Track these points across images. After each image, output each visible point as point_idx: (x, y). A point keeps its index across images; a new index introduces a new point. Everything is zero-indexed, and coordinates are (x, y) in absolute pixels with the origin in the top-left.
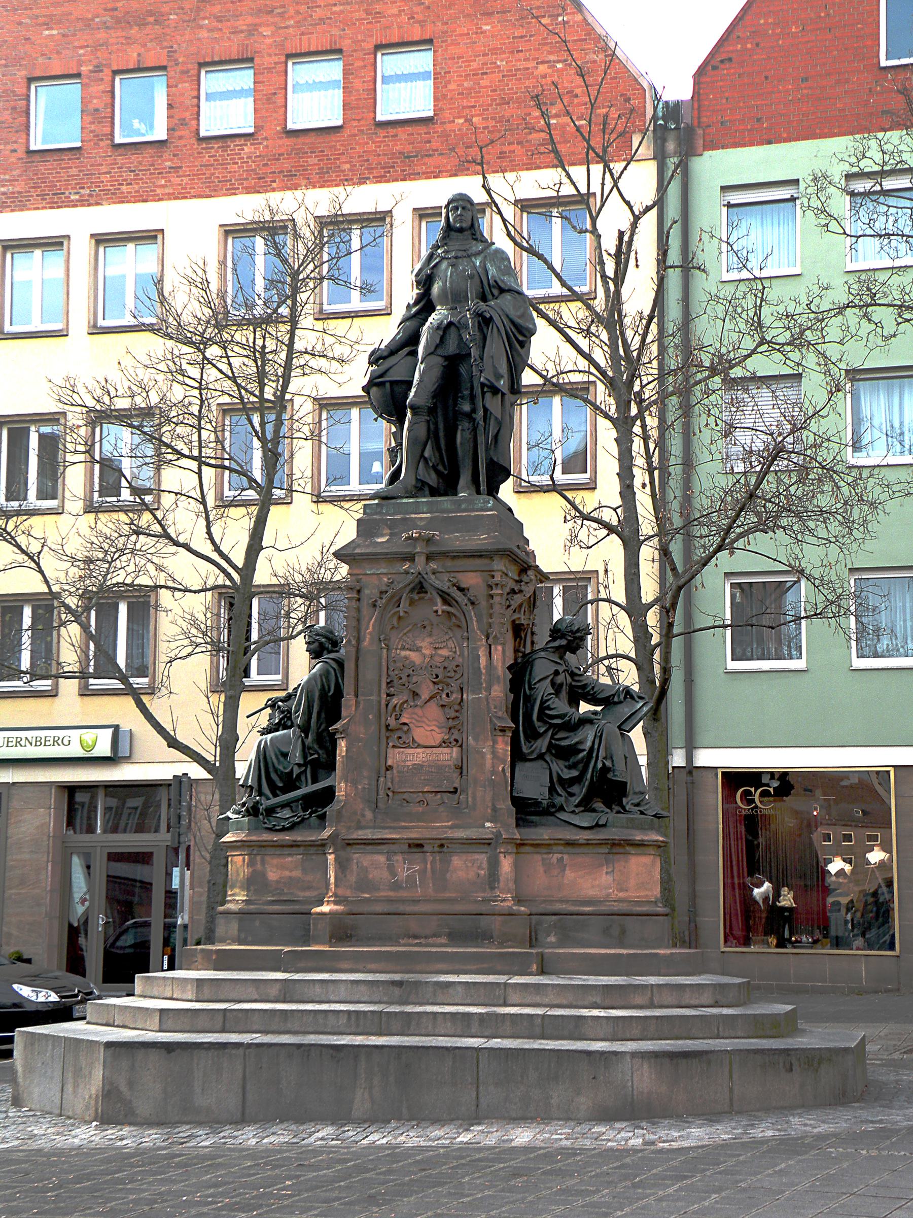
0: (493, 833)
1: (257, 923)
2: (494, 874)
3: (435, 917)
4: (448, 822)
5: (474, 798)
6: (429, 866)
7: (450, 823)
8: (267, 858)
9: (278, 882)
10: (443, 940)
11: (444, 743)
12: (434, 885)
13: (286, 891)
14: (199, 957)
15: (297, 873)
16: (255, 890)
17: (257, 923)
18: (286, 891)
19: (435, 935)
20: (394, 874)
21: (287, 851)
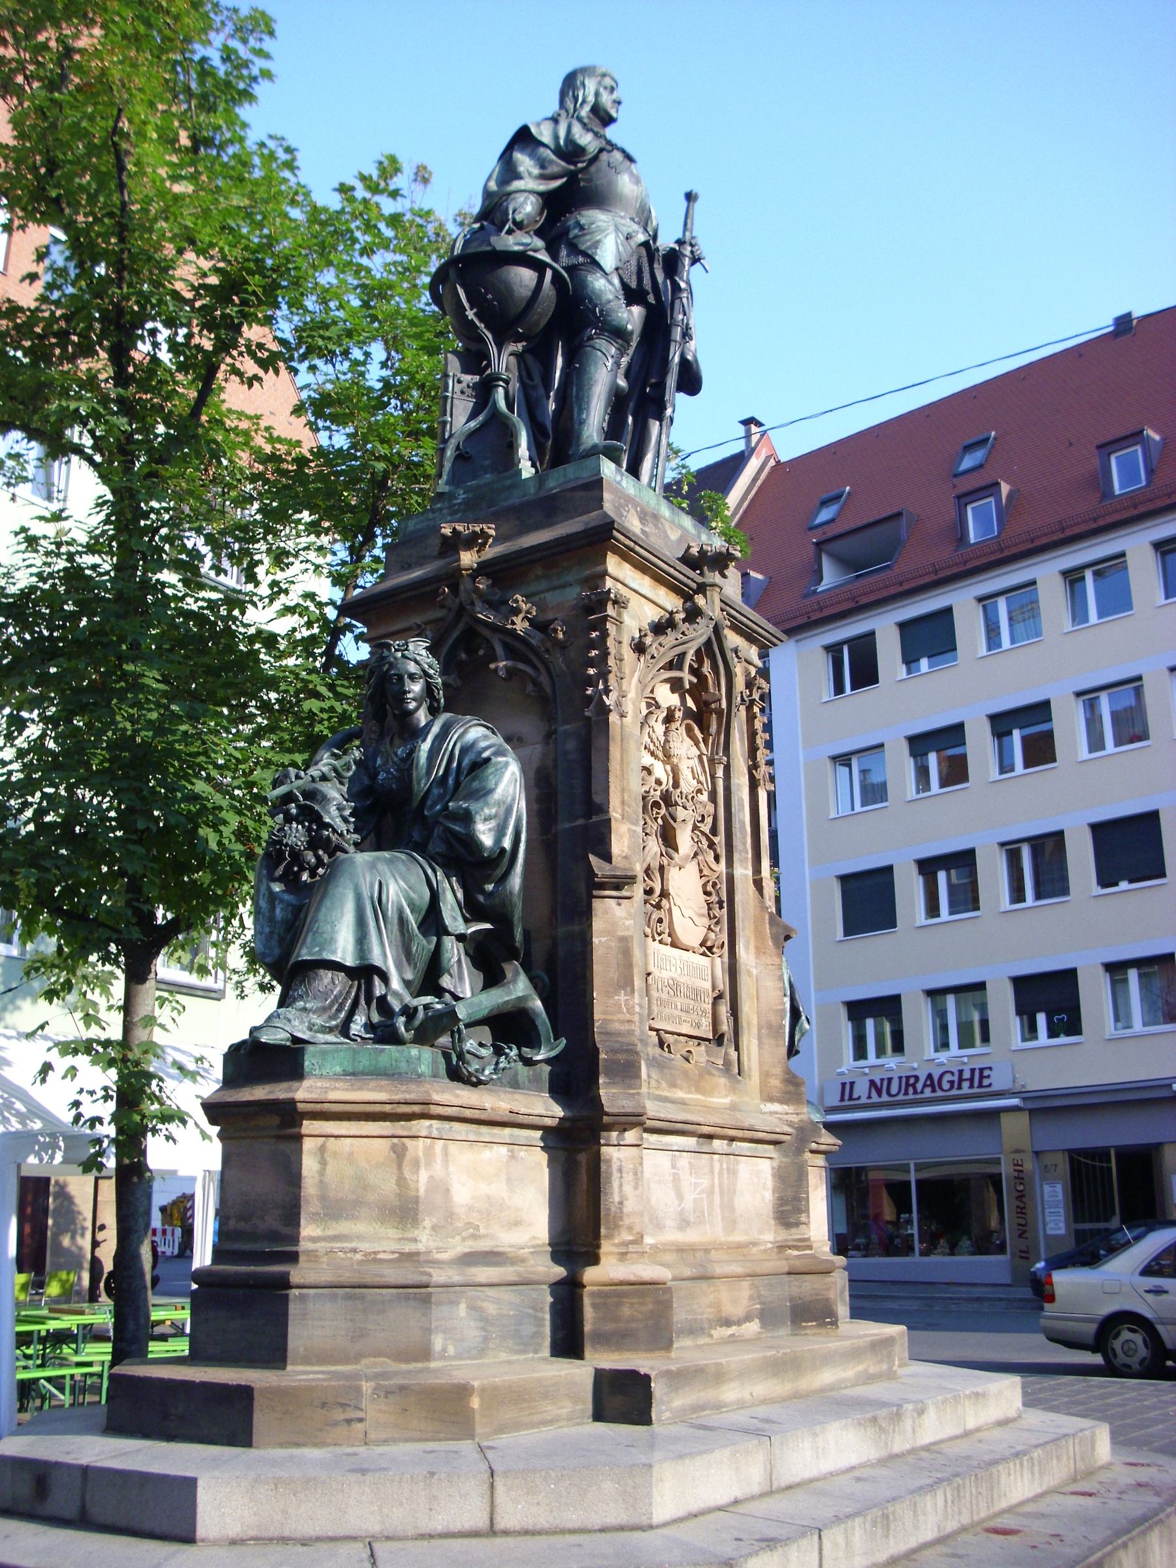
0: (790, 1124)
1: (462, 1309)
2: (797, 1199)
3: (746, 1284)
4: (726, 1096)
5: (749, 1060)
6: (716, 1181)
7: (727, 1101)
8: (453, 1147)
9: (471, 1208)
10: (753, 1327)
11: (708, 949)
12: (723, 1219)
13: (482, 1231)
14: (374, 1410)
15: (498, 1189)
16: (434, 1228)
17: (462, 1309)
18: (482, 1231)
19: (748, 1318)
20: (680, 1197)
21: (486, 1132)
